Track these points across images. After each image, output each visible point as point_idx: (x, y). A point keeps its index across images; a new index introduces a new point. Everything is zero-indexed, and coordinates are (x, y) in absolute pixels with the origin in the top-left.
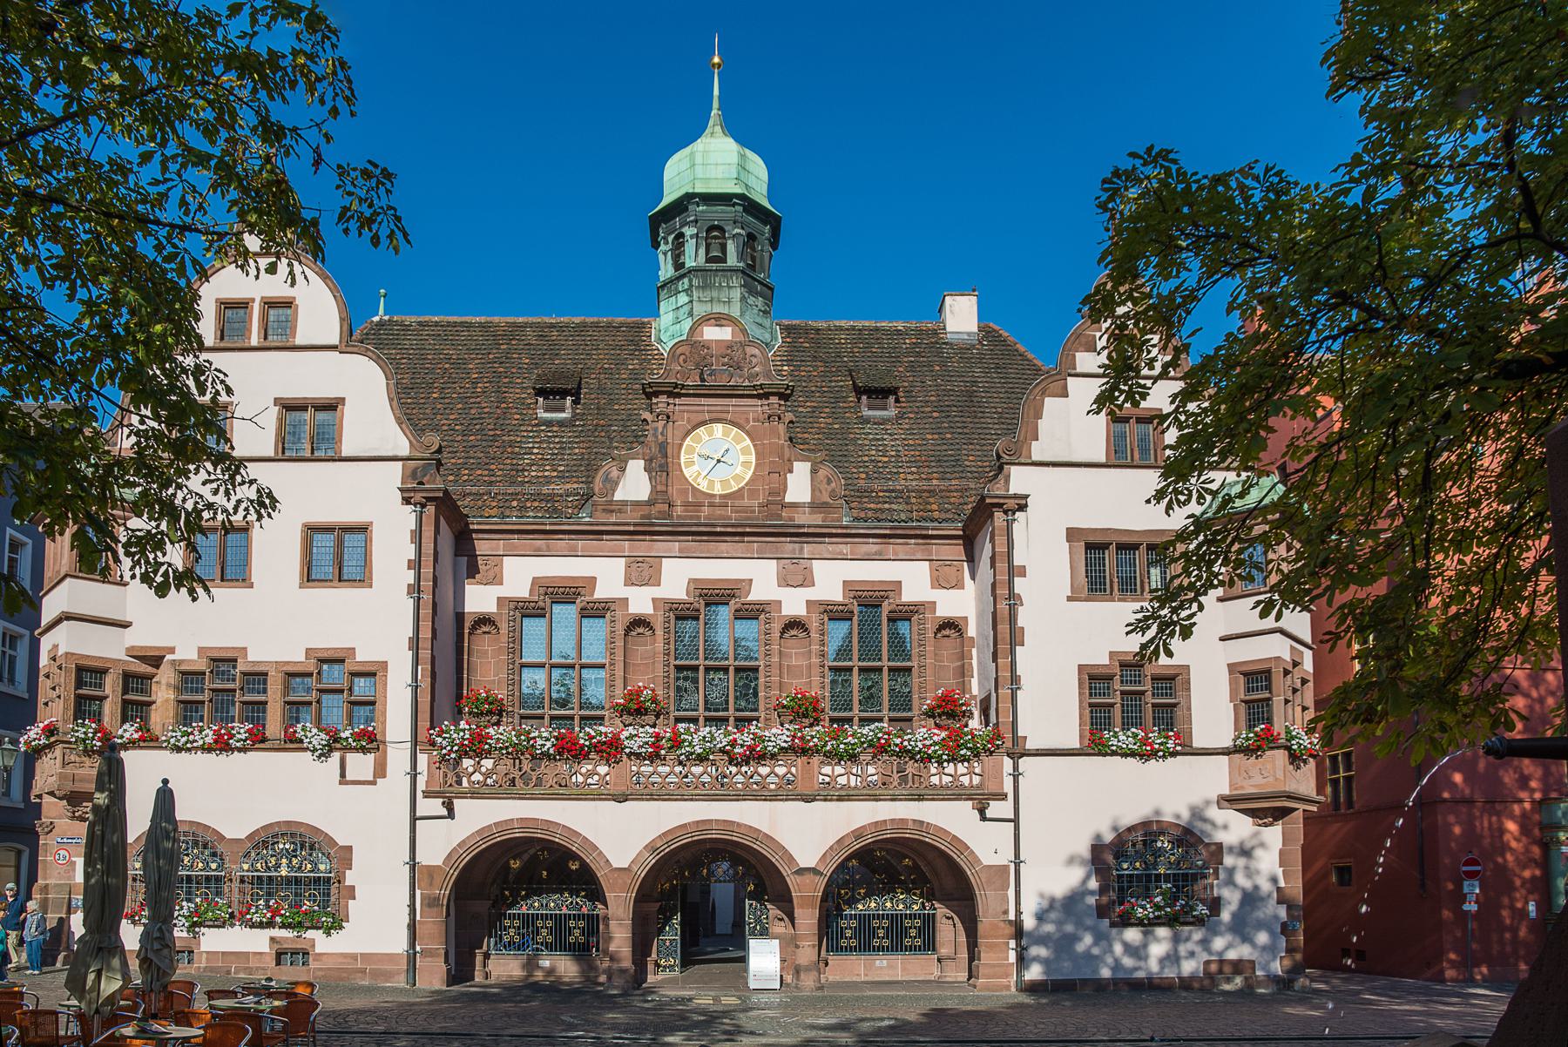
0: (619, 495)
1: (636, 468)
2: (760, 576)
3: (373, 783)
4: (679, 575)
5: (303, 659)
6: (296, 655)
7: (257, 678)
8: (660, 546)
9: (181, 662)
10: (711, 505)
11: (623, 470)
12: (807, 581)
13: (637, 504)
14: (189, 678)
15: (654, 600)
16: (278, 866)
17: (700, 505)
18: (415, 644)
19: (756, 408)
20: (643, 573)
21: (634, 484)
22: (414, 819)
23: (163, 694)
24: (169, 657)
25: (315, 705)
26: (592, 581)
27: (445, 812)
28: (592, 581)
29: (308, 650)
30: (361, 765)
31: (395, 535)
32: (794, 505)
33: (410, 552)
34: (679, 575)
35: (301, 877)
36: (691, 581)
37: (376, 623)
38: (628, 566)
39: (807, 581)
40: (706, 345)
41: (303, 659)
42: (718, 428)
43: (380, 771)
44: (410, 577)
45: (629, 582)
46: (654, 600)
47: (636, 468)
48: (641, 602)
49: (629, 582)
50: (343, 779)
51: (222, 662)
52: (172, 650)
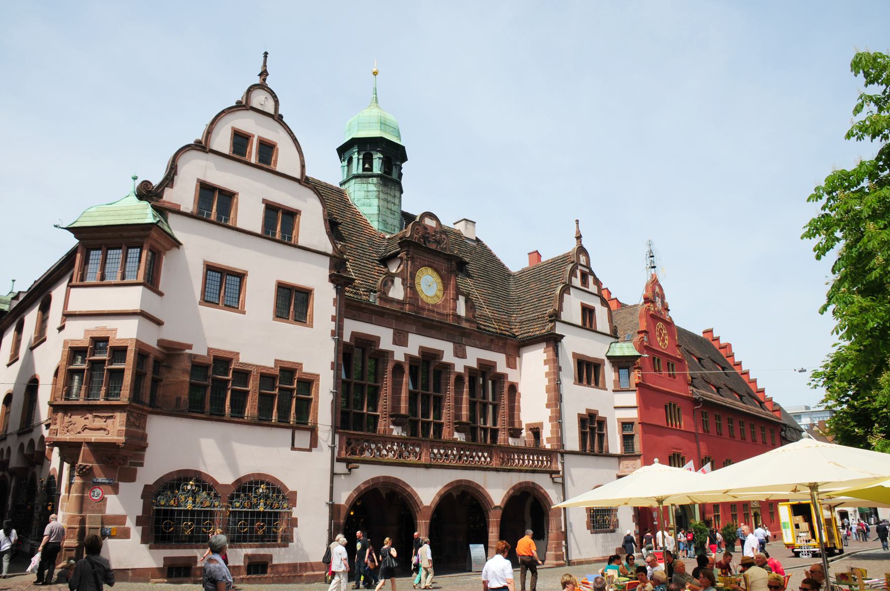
0: (391, 294)
1: (398, 281)
2: (446, 349)
3: (310, 450)
4: (416, 343)
5: (273, 366)
6: (267, 361)
7: (243, 375)
8: (407, 327)
9: (195, 356)
10: (429, 310)
11: (393, 282)
12: (464, 356)
13: (398, 302)
14: (198, 367)
15: (405, 355)
16: (257, 505)
17: (423, 309)
18: (335, 366)
19: (444, 266)
20: (400, 340)
21: (397, 292)
22: (333, 474)
23: (180, 378)
24: (188, 351)
25: (281, 398)
26: (378, 338)
27: (346, 471)
28: (378, 338)
29: (276, 361)
30: (303, 438)
31: (324, 300)
32: (459, 317)
33: (333, 311)
34: (416, 343)
35: (260, 510)
36: (421, 348)
37: (313, 350)
38: (394, 334)
39: (464, 356)
40: (425, 228)
41: (273, 366)
42: (430, 270)
43: (314, 443)
44: (332, 326)
45: (395, 342)
46: (405, 355)
47: (398, 281)
48: (399, 354)
49: (395, 342)
50: (293, 448)
51: (222, 361)
52: (190, 347)
